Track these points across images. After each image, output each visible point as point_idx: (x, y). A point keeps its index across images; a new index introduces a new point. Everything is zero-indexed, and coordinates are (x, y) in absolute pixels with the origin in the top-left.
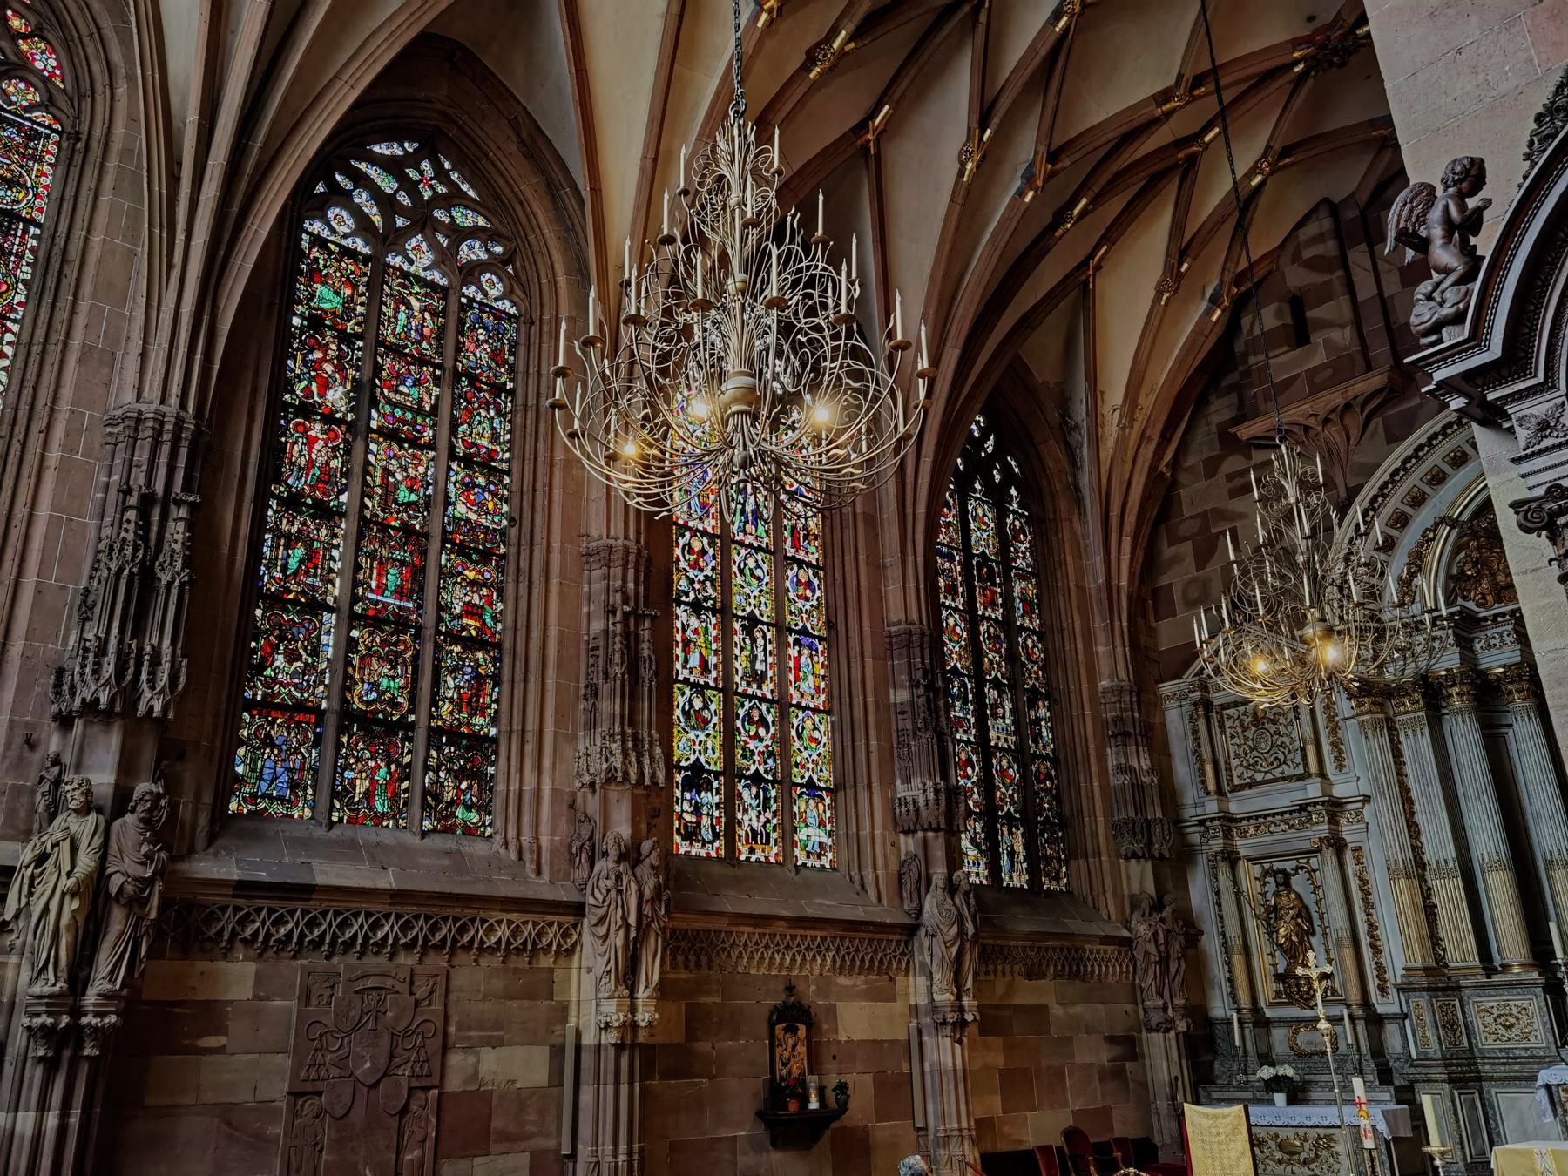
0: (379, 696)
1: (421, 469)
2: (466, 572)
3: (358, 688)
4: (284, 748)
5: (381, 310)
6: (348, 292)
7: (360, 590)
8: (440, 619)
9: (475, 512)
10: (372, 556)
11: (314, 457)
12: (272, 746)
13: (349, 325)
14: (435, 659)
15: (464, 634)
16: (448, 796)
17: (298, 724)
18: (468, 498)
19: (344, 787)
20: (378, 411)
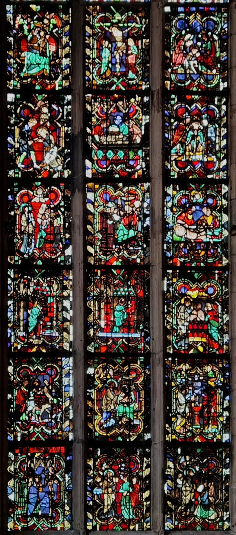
0: (117, 422)
1: (137, 204)
2: (189, 293)
3: (98, 418)
4: (43, 476)
5: (84, 54)
6: (53, 48)
7: (92, 332)
8: (167, 343)
9: (194, 231)
10: (99, 298)
11: (39, 221)
12: (34, 476)
13: (57, 82)
14: (165, 380)
15: (191, 352)
16: (187, 498)
17: (52, 455)
18: (185, 220)
19: (94, 502)
20: (92, 160)
